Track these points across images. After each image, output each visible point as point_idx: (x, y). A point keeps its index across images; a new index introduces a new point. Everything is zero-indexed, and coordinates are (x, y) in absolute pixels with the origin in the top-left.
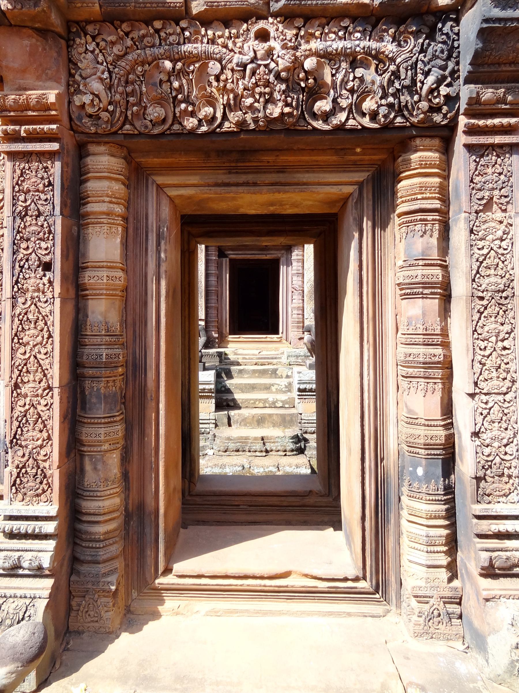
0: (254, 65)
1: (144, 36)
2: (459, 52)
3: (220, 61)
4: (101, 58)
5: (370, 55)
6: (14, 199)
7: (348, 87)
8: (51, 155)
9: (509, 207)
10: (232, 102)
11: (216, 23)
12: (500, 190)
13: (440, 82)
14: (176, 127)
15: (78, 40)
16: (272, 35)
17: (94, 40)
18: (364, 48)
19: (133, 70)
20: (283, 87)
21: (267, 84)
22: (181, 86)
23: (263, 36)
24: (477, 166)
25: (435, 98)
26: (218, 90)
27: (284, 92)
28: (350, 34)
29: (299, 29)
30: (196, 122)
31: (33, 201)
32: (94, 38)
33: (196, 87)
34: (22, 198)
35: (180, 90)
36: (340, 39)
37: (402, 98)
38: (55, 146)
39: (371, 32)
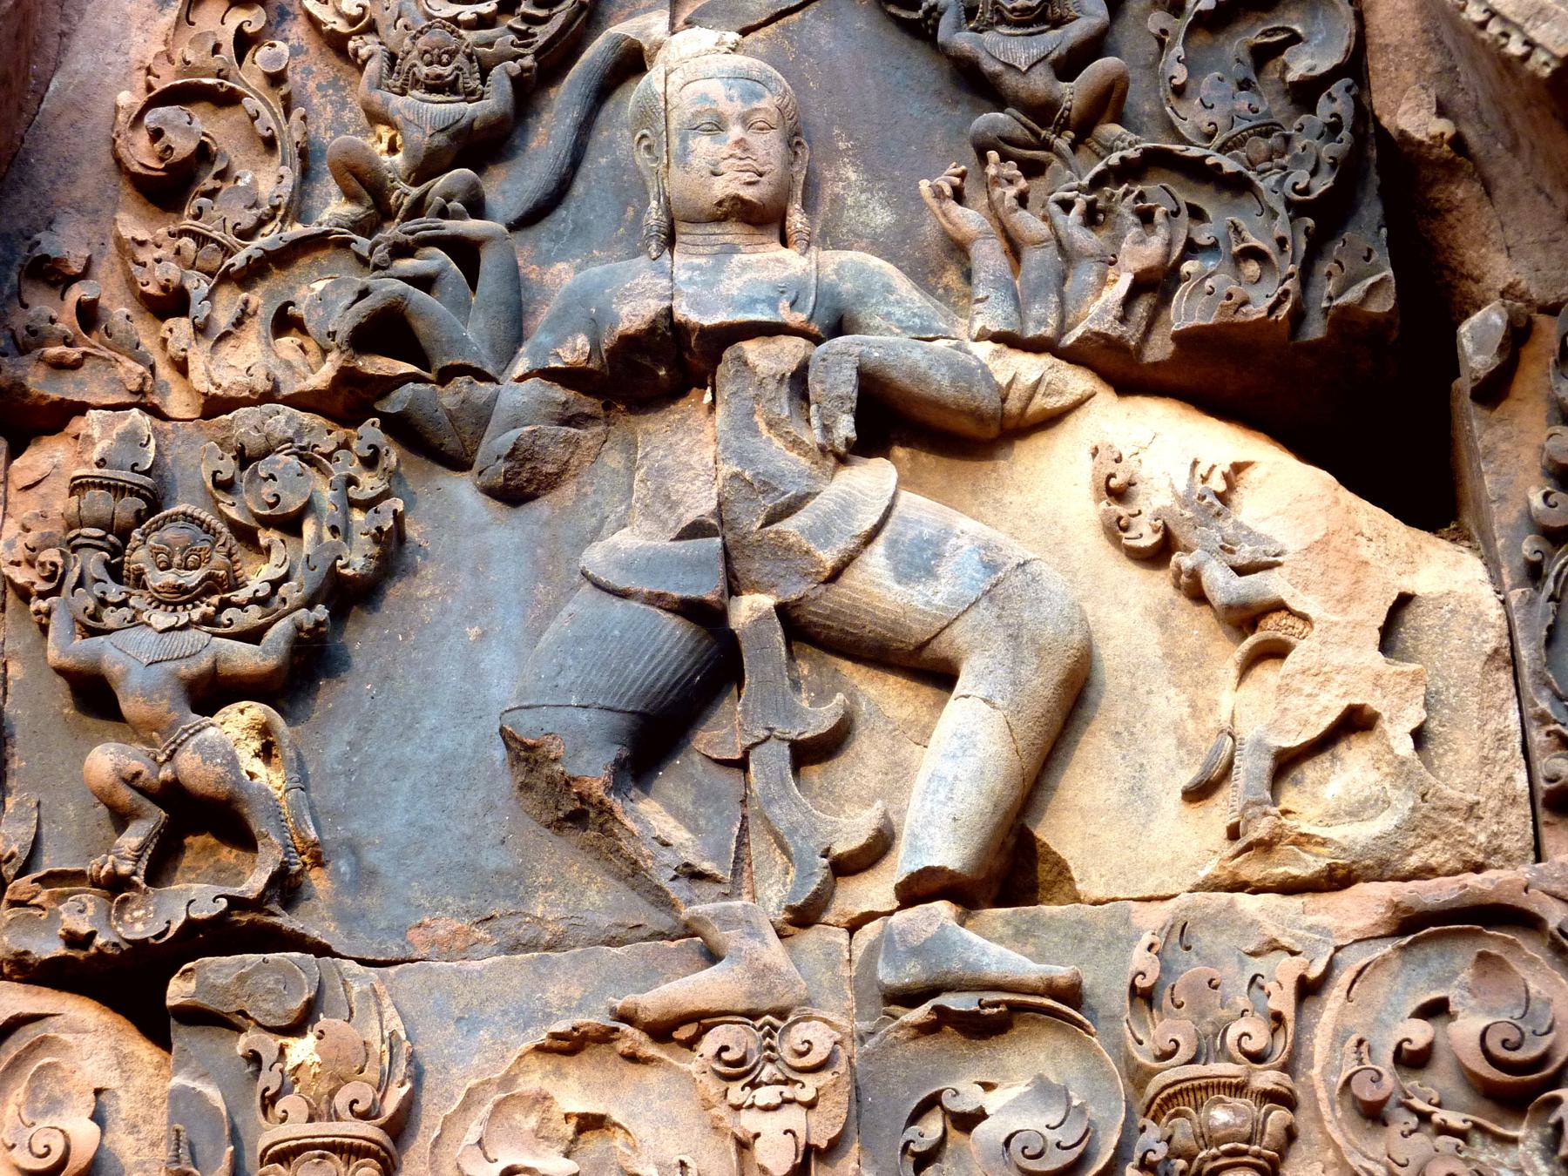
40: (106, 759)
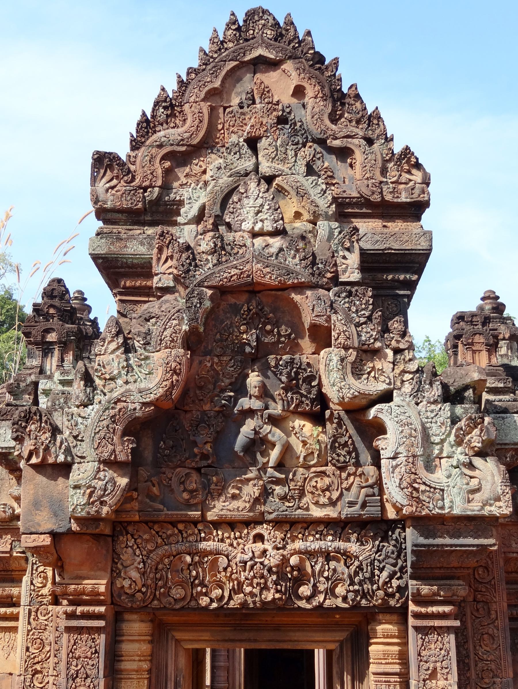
0: (252, 562)
1: (171, 535)
2: (406, 553)
3: (227, 556)
4: (138, 552)
5: (339, 553)
6: (68, 664)
7: (325, 576)
8: (98, 630)
9: (449, 676)
10: (236, 587)
11: (224, 525)
12: (442, 662)
13: (391, 576)
14: (193, 603)
15: (121, 538)
16: (266, 538)
17: (133, 538)
18: (335, 548)
19: (162, 561)
20: (274, 577)
21: (262, 576)
22: (198, 573)
23: (259, 538)
24: (423, 642)
25: (389, 588)
26: (226, 577)
27: (274, 581)
28: (325, 536)
29: (287, 532)
30: (208, 600)
31: (82, 666)
32: (132, 536)
33: (209, 574)
34: (74, 663)
35: (196, 578)
36: (317, 539)
37: (365, 586)
38: (101, 623)
39: (340, 534)
40: (196, 450)
